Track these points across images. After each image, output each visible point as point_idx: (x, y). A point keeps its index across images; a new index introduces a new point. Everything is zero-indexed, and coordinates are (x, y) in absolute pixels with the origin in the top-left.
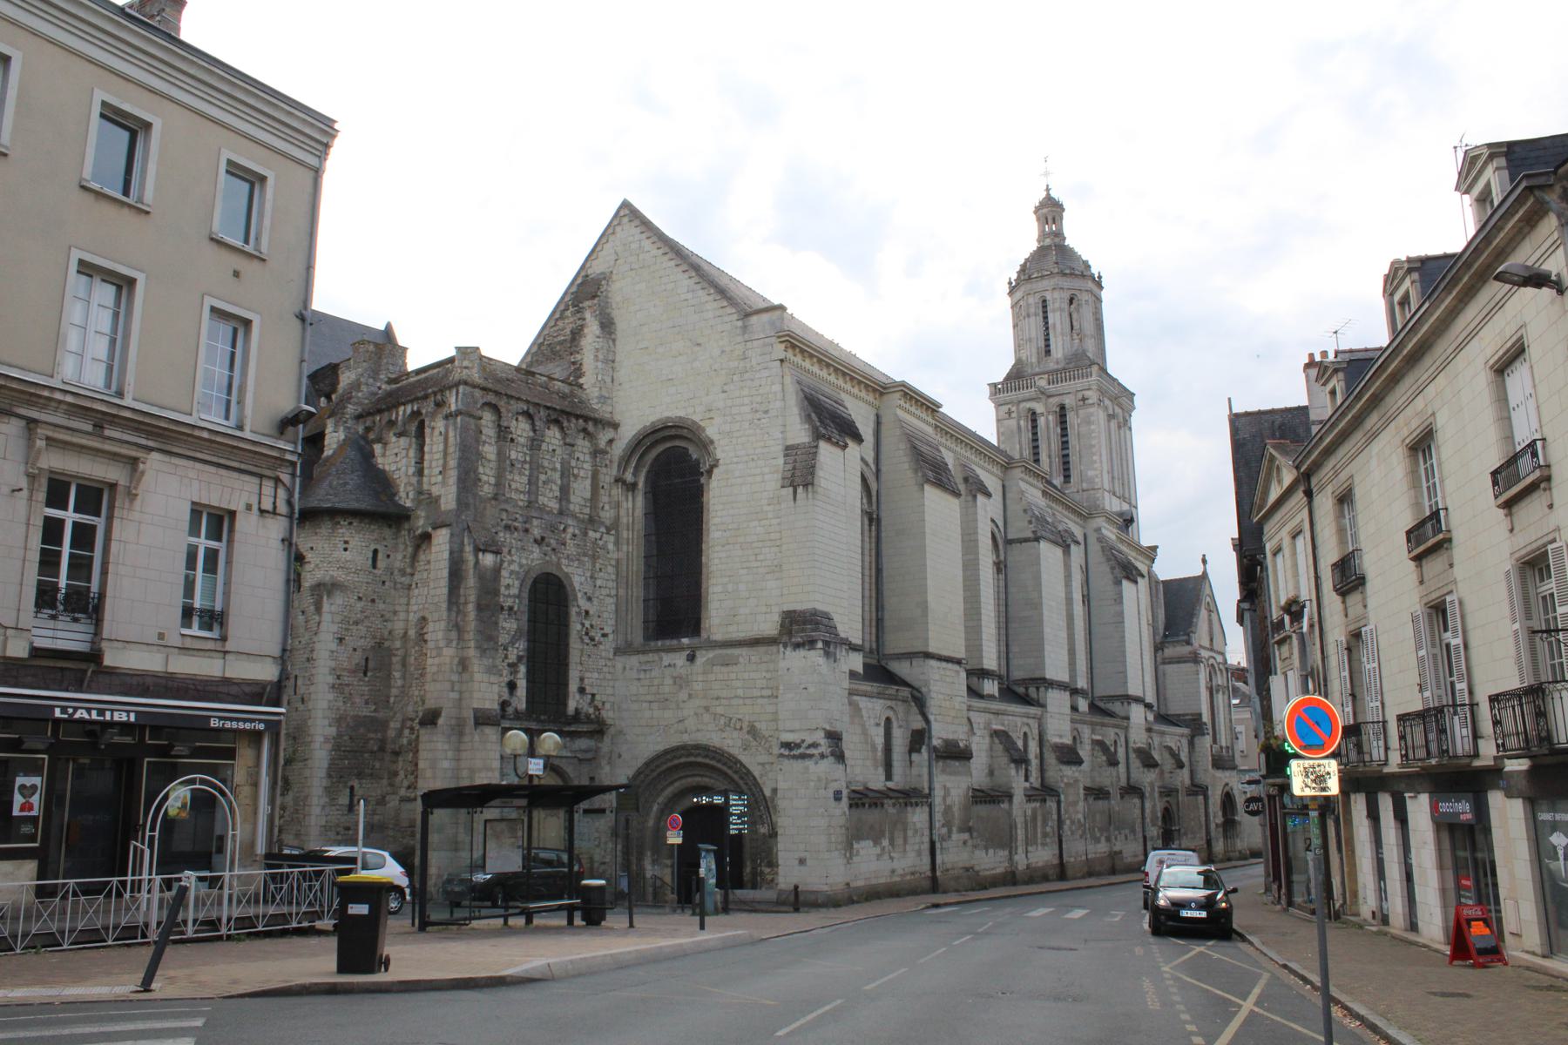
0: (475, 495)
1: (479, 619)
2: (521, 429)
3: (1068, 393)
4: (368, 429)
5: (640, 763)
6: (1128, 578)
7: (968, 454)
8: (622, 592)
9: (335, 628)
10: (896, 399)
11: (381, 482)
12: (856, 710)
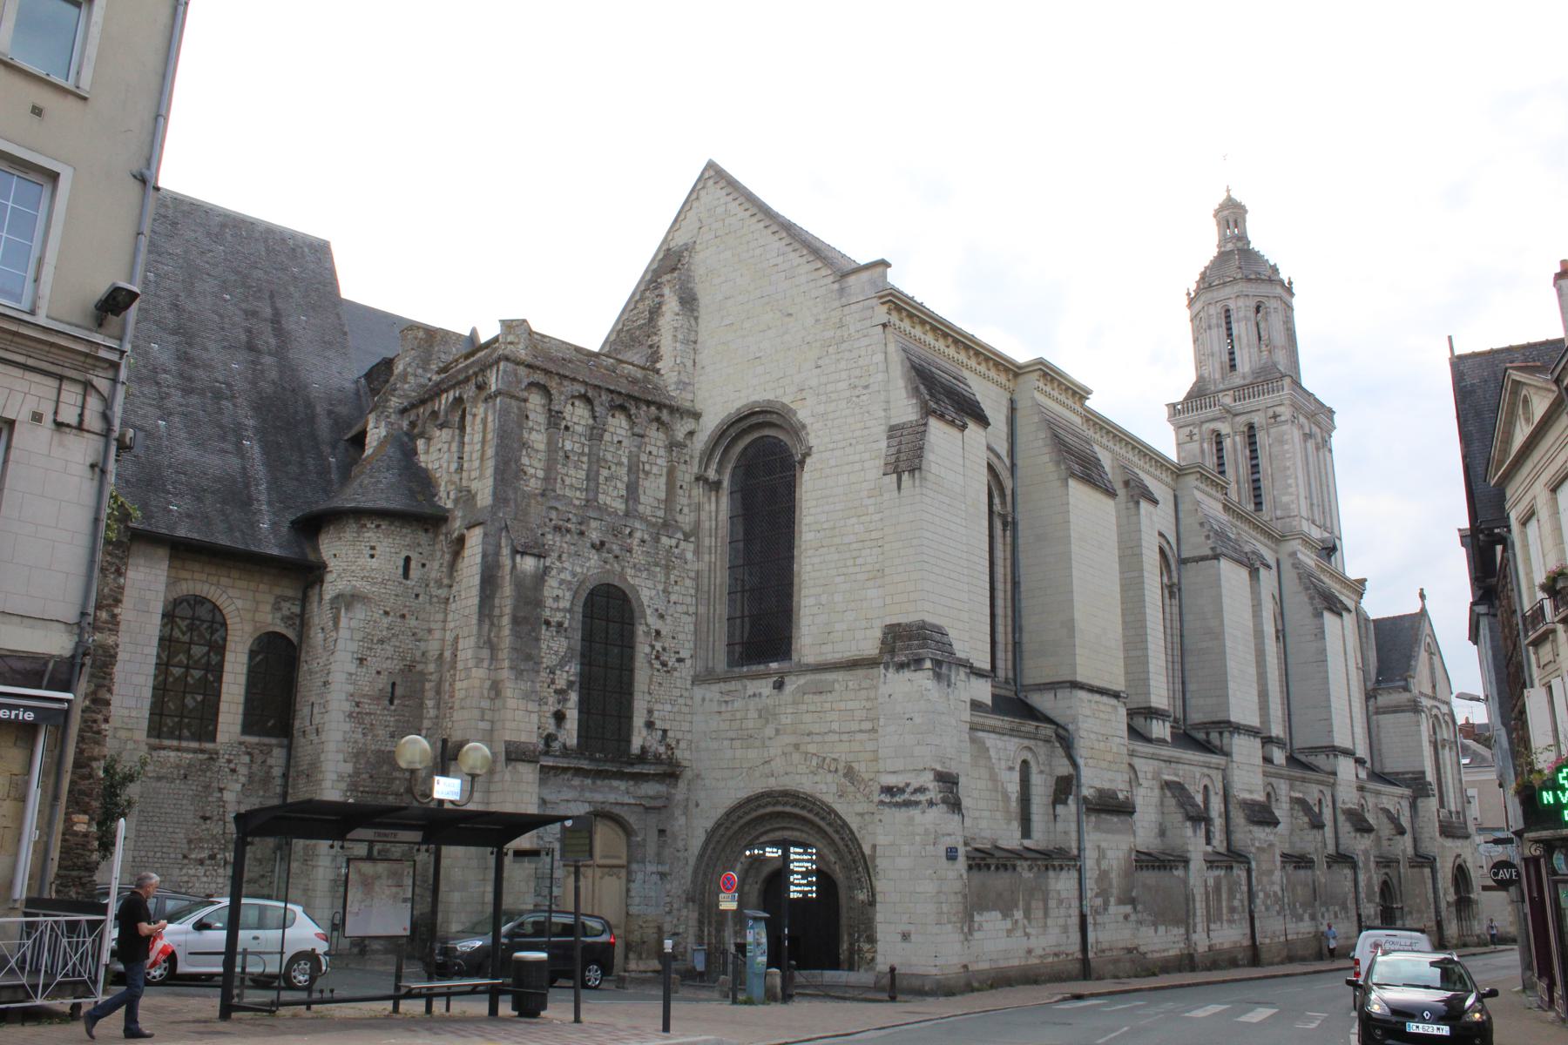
0: (516, 490)
1: (516, 634)
2: (578, 415)
3: (1257, 408)
4: (413, 424)
5: (721, 812)
6: (1331, 610)
7: (1130, 455)
8: (702, 610)
9: (353, 646)
10: (1033, 380)
11: (423, 482)
12: (981, 750)
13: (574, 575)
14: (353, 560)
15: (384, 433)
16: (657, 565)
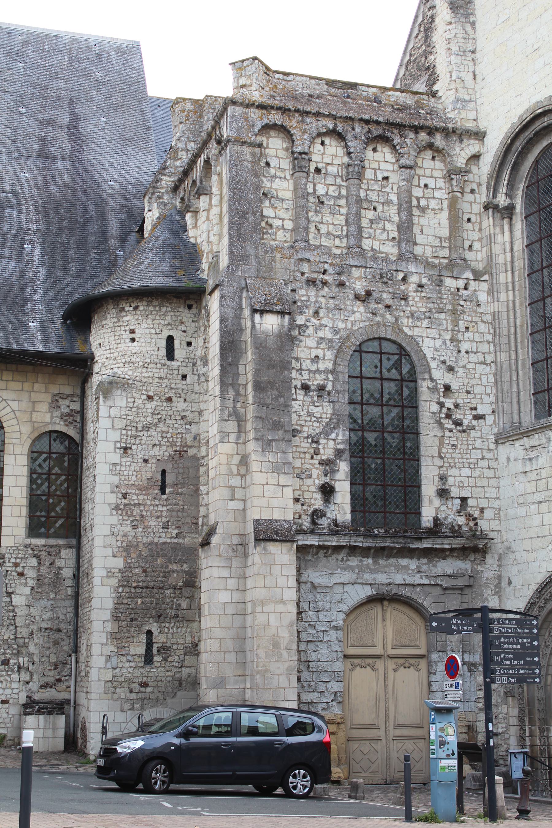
1: (260, 404)
5: (533, 588)
8: (503, 357)
9: (116, 436)
13: (336, 331)
14: (121, 345)
15: (158, 215)
16: (441, 311)
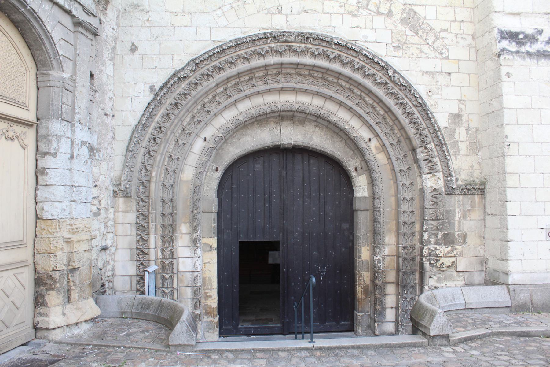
5: (180, 61)
